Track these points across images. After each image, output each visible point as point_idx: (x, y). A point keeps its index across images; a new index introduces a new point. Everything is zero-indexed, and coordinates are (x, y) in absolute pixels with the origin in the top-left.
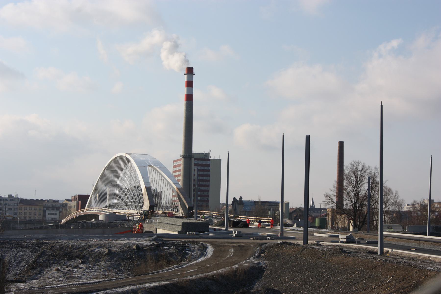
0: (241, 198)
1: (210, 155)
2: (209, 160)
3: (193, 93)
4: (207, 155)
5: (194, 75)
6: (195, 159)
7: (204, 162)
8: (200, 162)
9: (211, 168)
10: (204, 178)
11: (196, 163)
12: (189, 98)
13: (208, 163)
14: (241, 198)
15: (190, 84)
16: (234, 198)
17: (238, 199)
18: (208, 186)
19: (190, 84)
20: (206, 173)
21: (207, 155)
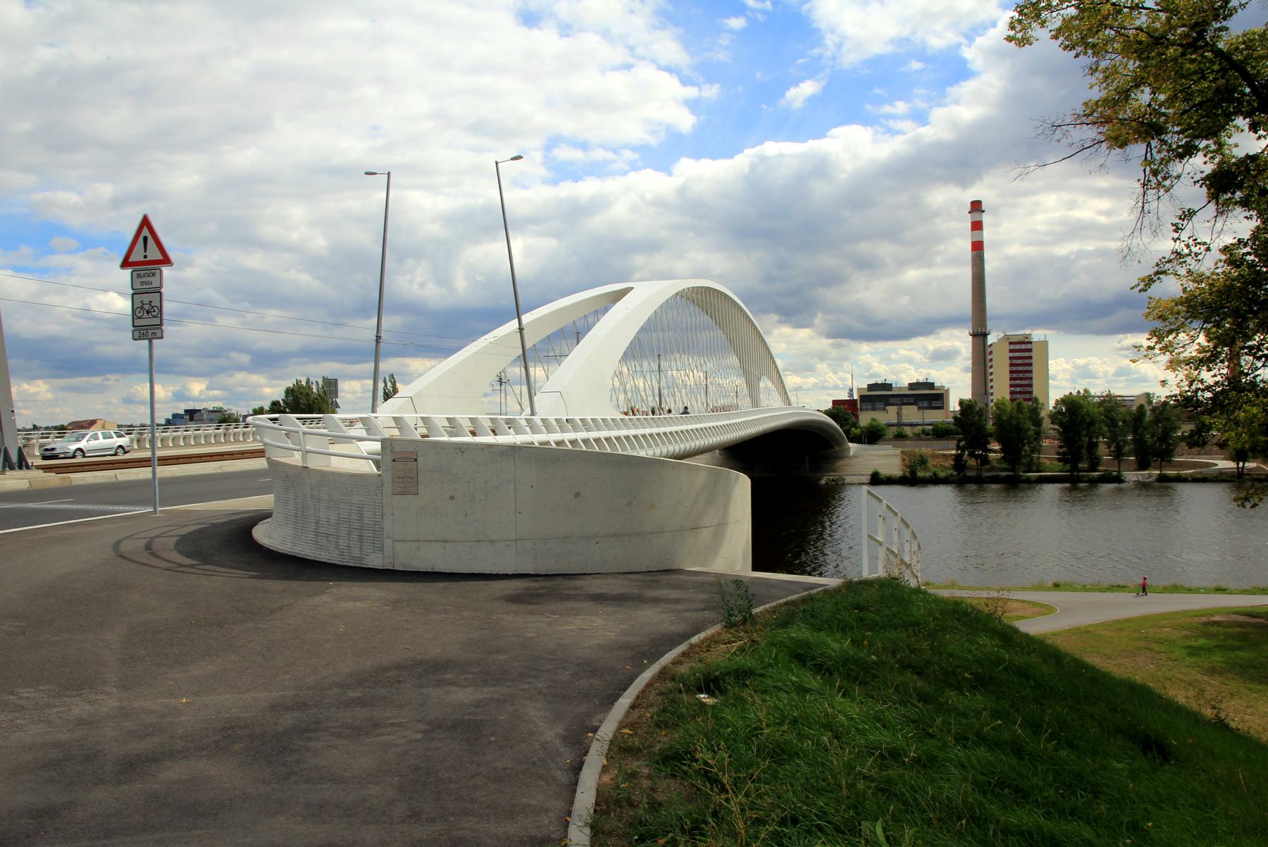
1: (1032, 336)
2: (1031, 343)
5: (984, 211)
6: (1011, 343)
7: (1023, 347)
8: (1018, 347)
11: (1011, 348)
12: (978, 247)
13: (1029, 346)
15: (977, 226)
18: (1031, 378)
19: (977, 226)
20: (1027, 361)
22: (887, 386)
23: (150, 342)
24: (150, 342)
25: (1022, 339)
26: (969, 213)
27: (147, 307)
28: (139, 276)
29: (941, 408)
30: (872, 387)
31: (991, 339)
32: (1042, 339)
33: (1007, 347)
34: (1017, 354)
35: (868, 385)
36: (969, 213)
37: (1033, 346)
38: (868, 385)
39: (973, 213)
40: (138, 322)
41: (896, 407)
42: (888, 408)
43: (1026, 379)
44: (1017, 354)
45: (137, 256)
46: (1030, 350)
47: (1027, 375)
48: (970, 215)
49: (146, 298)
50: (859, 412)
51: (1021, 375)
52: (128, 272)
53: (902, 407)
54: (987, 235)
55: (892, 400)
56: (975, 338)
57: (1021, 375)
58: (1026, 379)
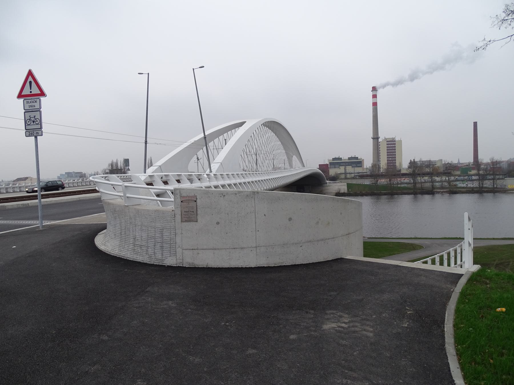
0: (414, 160)
1: (396, 138)
2: (395, 141)
3: (377, 101)
4: (393, 139)
6: (387, 141)
7: (392, 143)
8: (390, 143)
9: (396, 145)
10: (393, 151)
12: (375, 104)
14: (414, 160)
15: (375, 96)
16: (411, 160)
17: (412, 160)
19: (375, 96)
21: (394, 139)
22: (341, 159)
23: (36, 137)
24: (36, 137)
25: (391, 140)
26: (372, 91)
27: (33, 119)
28: (28, 102)
29: (361, 167)
30: (334, 159)
31: (380, 140)
32: (400, 140)
33: (386, 143)
34: (389, 146)
35: (333, 158)
36: (372, 91)
37: (396, 143)
38: (333, 158)
39: (373, 92)
40: (28, 127)
41: (344, 167)
42: (340, 167)
43: (393, 155)
44: (389, 146)
45: (26, 92)
46: (395, 144)
47: (394, 154)
48: (372, 92)
49: (32, 114)
50: (329, 169)
51: (391, 154)
52: (22, 100)
53: (346, 166)
54: (379, 100)
55: (342, 164)
56: (374, 139)
57: (391, 154)
58: (393, 155)
